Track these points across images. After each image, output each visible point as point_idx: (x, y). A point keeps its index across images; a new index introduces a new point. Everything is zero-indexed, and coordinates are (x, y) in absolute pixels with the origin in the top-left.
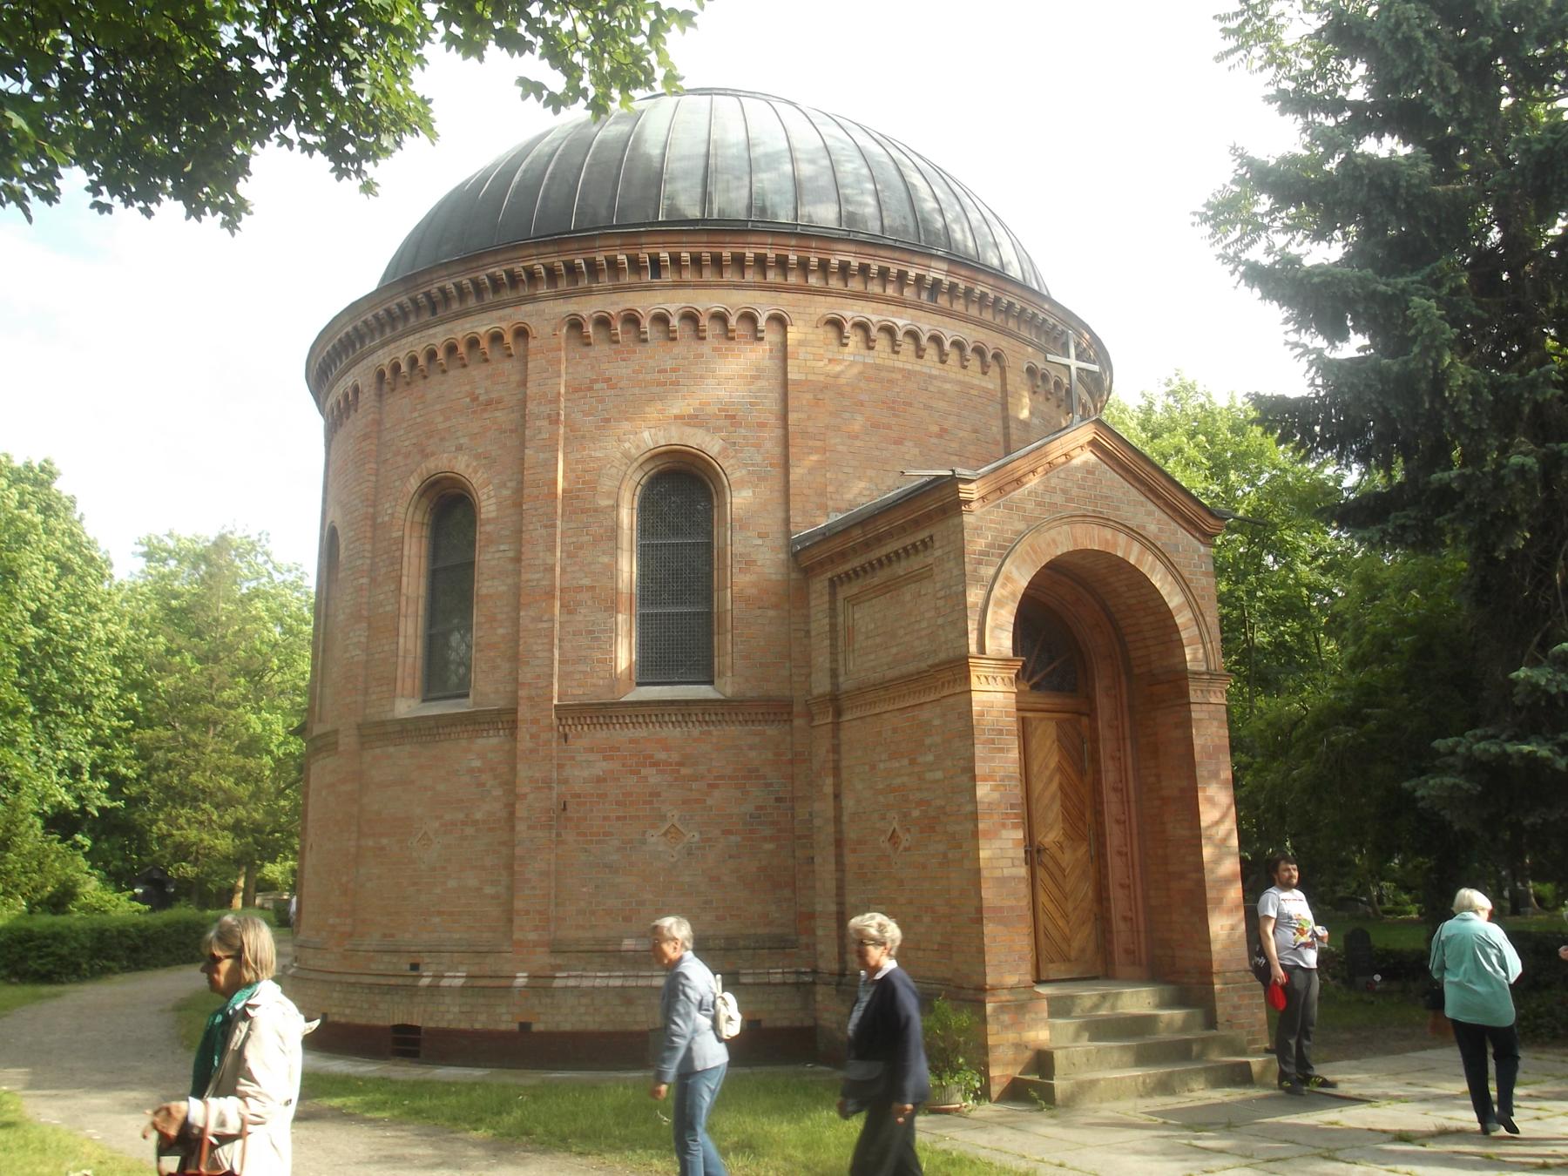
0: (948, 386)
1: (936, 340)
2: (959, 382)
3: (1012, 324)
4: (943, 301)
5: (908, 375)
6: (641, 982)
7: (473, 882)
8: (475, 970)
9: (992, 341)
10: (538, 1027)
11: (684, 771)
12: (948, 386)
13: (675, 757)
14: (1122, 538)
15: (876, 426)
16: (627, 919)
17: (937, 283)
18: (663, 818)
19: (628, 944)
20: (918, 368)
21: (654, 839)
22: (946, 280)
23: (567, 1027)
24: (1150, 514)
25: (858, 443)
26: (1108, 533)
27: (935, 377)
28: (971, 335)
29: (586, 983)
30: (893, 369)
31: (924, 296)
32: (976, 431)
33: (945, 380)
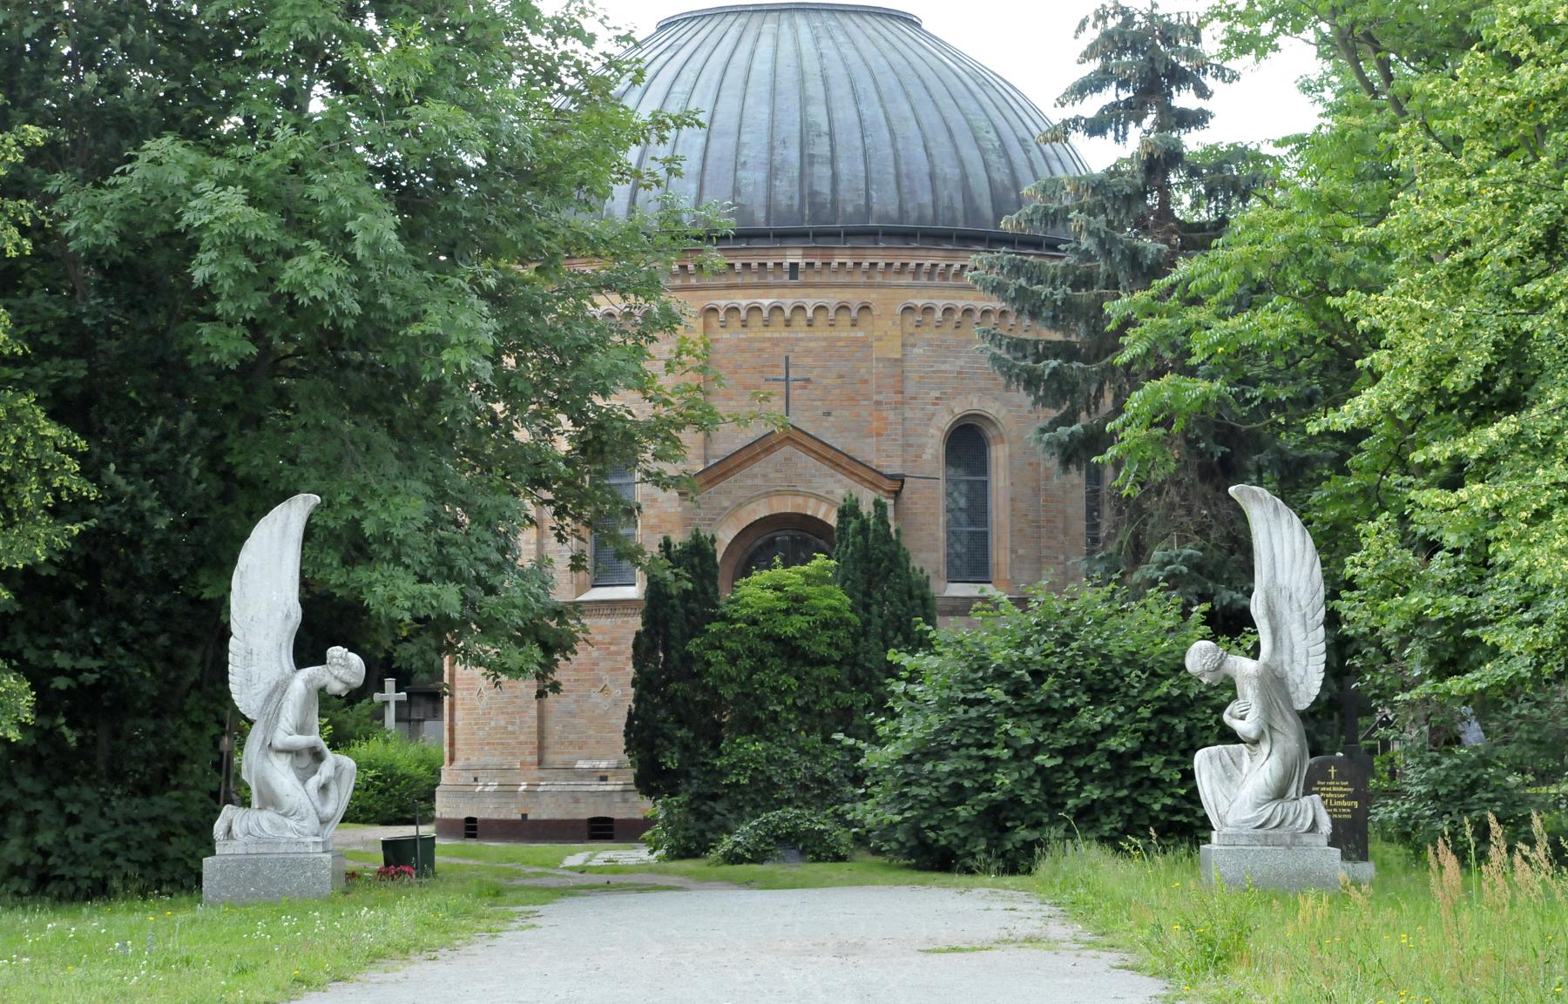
0: (812, 344)
1: (800, 308)
2: (825, 339)
3: (879, 279)
4: (801, 278)
5: (775, 342)
6: (584, 788)
7: (503, 723)
8: (503, 781)
9: (854, 297)
10: (530, 817)
11: (613, 648)
12: (812, 344)
13: (607, 639)
14: (812, 502)
15: (746, 388)
16: (581, 748)
17: (794, 266)
18: (600, 680)
19: (581, 764)
20: (785, 335)
21: (596, 697)
22: (802, 262)
23: (544, 817)
24: (839, 481)
25: (732, 403)
26: (800, 500)
27: (801, 339)
28: (831, 298)
29: (554, 789)
30: (764, 340)
31: (786, 277)
32: (841, 376)
33: (810, 340)
